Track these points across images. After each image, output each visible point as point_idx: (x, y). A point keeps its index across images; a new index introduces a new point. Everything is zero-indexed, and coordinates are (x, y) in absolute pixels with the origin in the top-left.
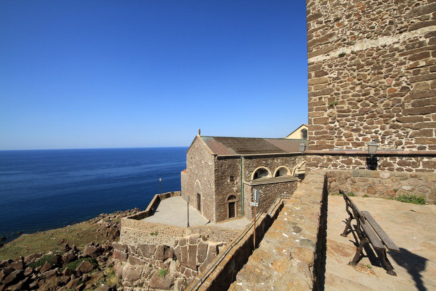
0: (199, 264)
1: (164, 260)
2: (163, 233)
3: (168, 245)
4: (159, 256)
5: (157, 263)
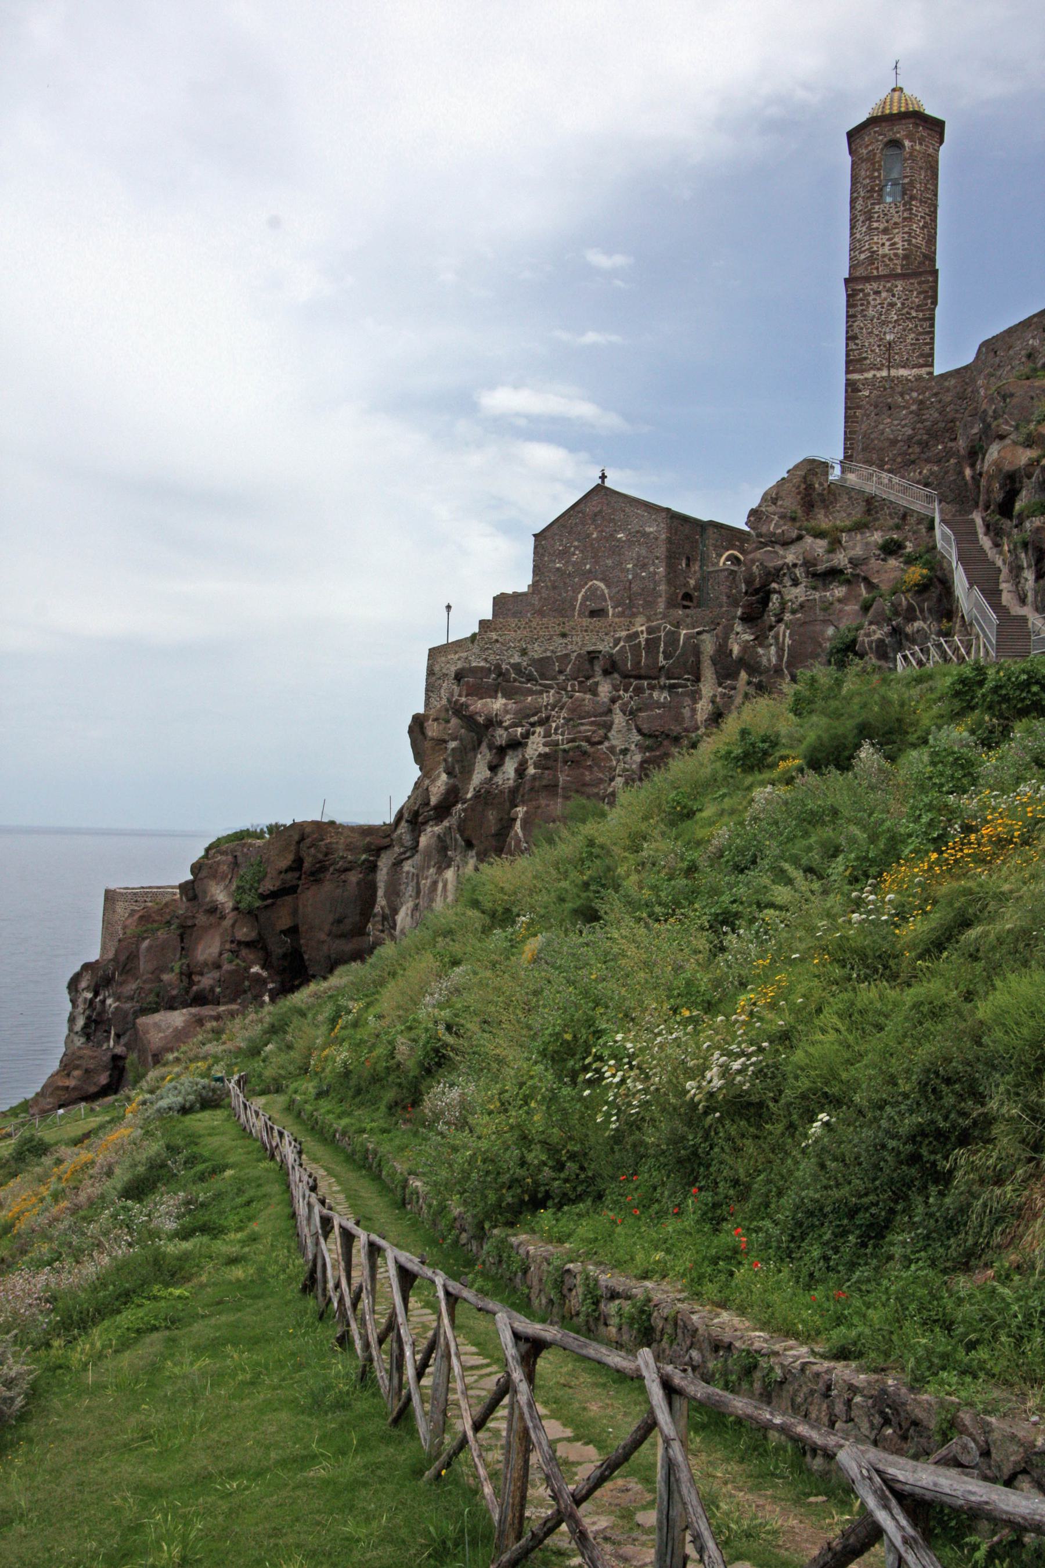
0: (664, 662)
1: (588, 678)
2: (586, 631)
3: (601, 648)
4: (579, 670)
5: (573, 686)
